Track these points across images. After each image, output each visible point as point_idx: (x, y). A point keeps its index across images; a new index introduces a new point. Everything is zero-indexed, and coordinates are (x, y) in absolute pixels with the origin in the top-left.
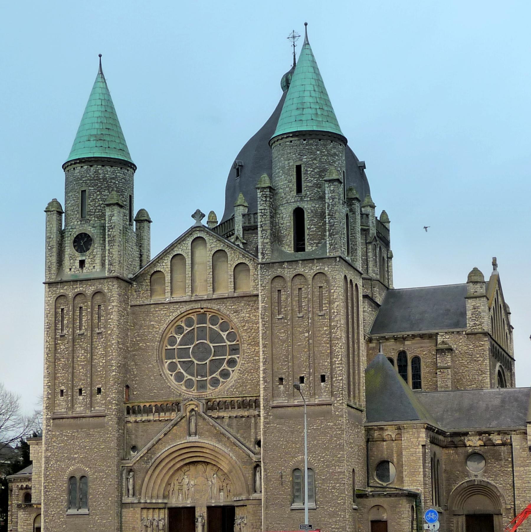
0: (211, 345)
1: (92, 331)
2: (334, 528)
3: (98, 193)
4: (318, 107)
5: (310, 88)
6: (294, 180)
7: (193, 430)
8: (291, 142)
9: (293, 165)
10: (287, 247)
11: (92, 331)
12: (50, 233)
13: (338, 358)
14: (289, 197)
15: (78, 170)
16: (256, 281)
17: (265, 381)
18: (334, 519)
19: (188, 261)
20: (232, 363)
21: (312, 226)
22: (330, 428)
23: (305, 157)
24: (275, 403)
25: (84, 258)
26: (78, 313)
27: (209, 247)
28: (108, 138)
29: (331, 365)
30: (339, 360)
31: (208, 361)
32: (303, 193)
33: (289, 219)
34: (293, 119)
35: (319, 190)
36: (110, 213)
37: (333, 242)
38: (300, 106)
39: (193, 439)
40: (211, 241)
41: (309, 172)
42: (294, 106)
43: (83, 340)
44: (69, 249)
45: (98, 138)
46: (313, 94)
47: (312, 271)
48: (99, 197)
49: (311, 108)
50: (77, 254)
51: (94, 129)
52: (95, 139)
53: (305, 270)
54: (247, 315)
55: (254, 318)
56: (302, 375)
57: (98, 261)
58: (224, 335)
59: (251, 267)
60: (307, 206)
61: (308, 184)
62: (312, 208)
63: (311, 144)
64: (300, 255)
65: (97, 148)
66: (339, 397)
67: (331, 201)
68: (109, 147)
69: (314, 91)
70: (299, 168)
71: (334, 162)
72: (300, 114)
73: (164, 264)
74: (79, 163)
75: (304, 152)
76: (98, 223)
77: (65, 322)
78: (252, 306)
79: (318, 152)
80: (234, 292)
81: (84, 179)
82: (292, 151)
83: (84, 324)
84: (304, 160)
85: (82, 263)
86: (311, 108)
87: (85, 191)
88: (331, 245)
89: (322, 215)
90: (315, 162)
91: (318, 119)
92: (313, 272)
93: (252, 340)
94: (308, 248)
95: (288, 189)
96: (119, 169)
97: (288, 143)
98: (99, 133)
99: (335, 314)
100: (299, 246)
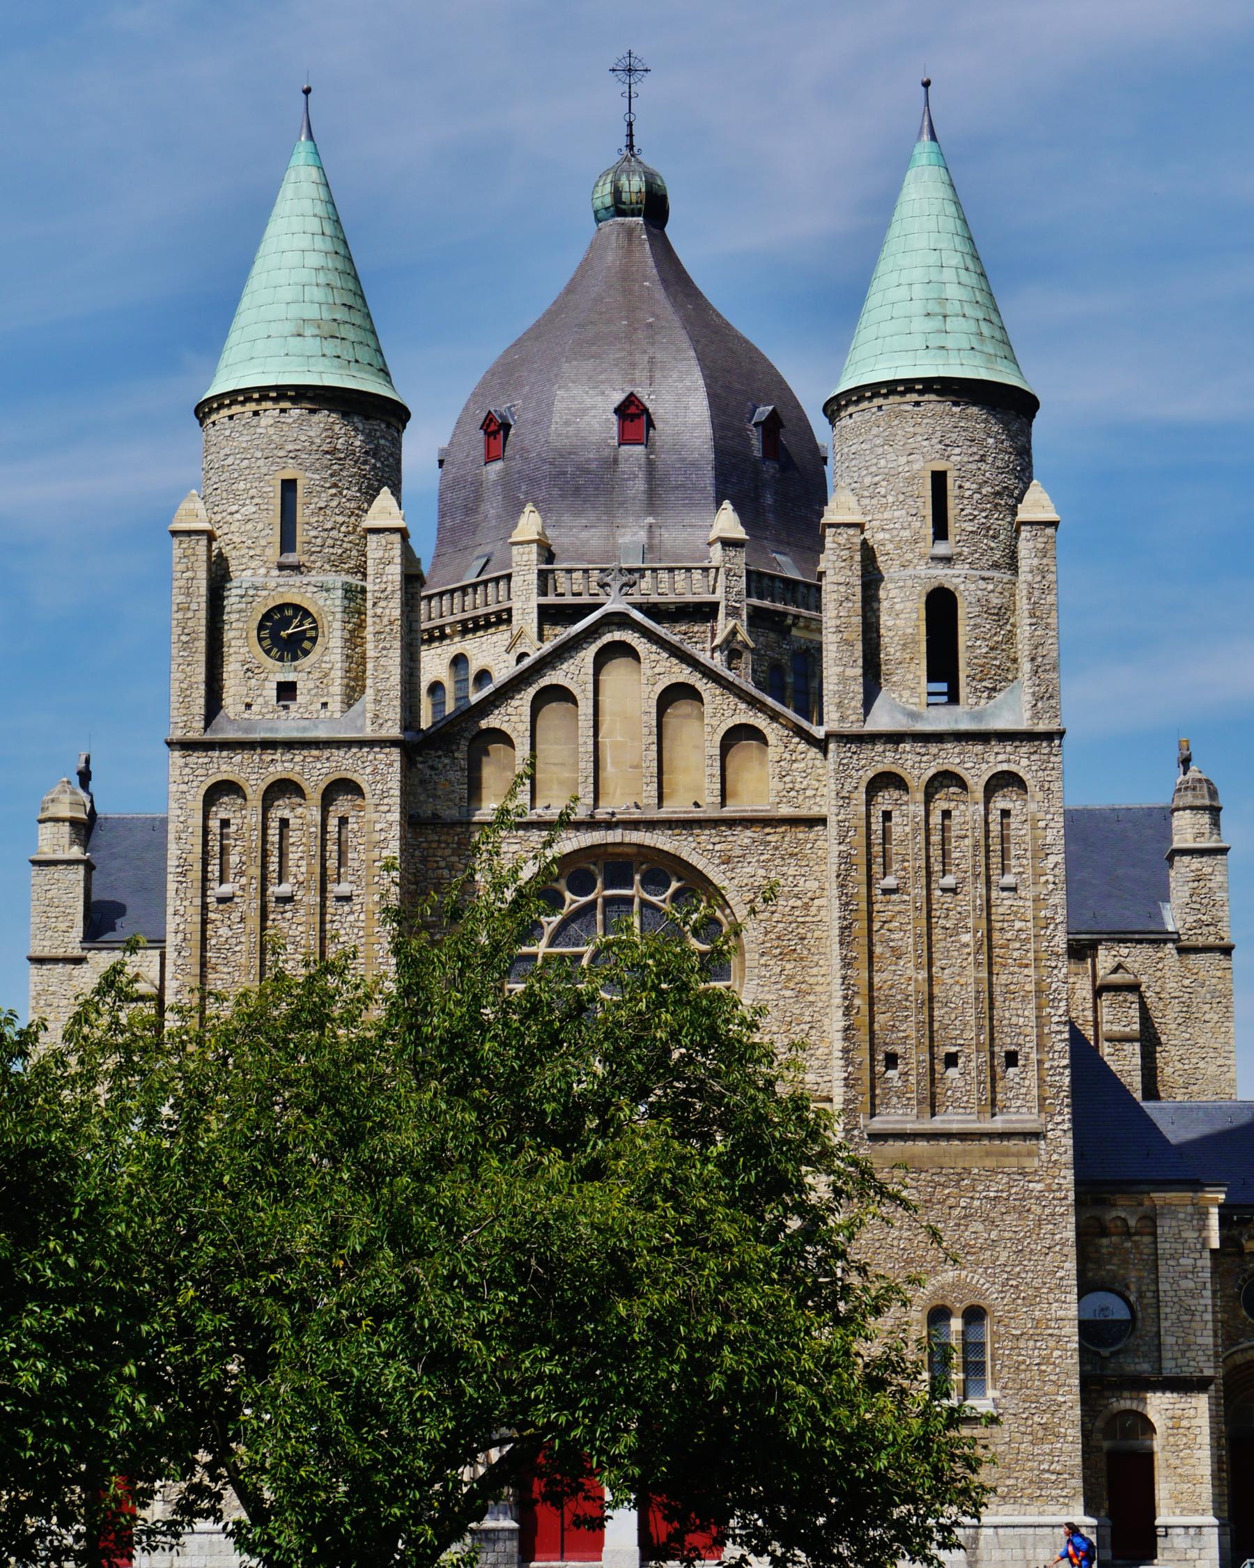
1: (323, 890)
2: (1048, 1471)
3: (333, 491)
4: (981, 316)
6: (928, 512)
8: (917, 404)
9: (923, 469)
10: (906, 694)
11: (323, 890)
12: (188, 595)
13: (1058, 1008)
14: (909, 556)
16: (787, 779)
17: (848, 1062)
18: (1047, 1448)
19: (586, 707)
21: (978, 643)
22: (1038, 1198)
23: (957, 451)
24: (878, 1124)
25: (291, 677)
26: (274, 837)
27: (649, 672)
29: (1040, 1026)
30: (1060, 1012)
33: (914, 616)
34: (919, 342)
35: (993, 545)
36: (380, 554)
37: (1043, 689)
38: (933, 307)
40: (653, 657)
41: (968, 493)
42: (917, 307)
43: (288, 915)
45: (326, 330)
47: (984, 766)
48: (334, 504)
49: (964, 316)
50: (269, 663)
51: (312, 302)
52: (316, 332)
53: (962, 762)
54: (762, 872)
56: (953, 1049)
57: (337, 688)
59: (771, 739)
61: (964, 525)
62: (979, 592)
65: (326, 360)
66: (1060, 1114)
67: (1038, 578)
68: (357, 361)
69: (967, 269)
70: (939, 479)
72: (939, 331)
73: (510, 710)
74: (276, 400)
75: (954, 436)
76: (337, 580)
77: (234, 859)
78: (776, 848)
79: (991, 441)
80: (723, 804)
81: (290, 447)
82: (918, 430)
83: (294, 870)
84: (953, 458)
85: (287, 691)
86: (964, 316)
87: (294, 481)
89: (1002, 614)
90: (984, 466)
91: (986, 350)
93: (775, 943)
95: (906, 534)
96: (383, 426)
97: (909, 408)
98: (327, 315)
99: (1051, 887)
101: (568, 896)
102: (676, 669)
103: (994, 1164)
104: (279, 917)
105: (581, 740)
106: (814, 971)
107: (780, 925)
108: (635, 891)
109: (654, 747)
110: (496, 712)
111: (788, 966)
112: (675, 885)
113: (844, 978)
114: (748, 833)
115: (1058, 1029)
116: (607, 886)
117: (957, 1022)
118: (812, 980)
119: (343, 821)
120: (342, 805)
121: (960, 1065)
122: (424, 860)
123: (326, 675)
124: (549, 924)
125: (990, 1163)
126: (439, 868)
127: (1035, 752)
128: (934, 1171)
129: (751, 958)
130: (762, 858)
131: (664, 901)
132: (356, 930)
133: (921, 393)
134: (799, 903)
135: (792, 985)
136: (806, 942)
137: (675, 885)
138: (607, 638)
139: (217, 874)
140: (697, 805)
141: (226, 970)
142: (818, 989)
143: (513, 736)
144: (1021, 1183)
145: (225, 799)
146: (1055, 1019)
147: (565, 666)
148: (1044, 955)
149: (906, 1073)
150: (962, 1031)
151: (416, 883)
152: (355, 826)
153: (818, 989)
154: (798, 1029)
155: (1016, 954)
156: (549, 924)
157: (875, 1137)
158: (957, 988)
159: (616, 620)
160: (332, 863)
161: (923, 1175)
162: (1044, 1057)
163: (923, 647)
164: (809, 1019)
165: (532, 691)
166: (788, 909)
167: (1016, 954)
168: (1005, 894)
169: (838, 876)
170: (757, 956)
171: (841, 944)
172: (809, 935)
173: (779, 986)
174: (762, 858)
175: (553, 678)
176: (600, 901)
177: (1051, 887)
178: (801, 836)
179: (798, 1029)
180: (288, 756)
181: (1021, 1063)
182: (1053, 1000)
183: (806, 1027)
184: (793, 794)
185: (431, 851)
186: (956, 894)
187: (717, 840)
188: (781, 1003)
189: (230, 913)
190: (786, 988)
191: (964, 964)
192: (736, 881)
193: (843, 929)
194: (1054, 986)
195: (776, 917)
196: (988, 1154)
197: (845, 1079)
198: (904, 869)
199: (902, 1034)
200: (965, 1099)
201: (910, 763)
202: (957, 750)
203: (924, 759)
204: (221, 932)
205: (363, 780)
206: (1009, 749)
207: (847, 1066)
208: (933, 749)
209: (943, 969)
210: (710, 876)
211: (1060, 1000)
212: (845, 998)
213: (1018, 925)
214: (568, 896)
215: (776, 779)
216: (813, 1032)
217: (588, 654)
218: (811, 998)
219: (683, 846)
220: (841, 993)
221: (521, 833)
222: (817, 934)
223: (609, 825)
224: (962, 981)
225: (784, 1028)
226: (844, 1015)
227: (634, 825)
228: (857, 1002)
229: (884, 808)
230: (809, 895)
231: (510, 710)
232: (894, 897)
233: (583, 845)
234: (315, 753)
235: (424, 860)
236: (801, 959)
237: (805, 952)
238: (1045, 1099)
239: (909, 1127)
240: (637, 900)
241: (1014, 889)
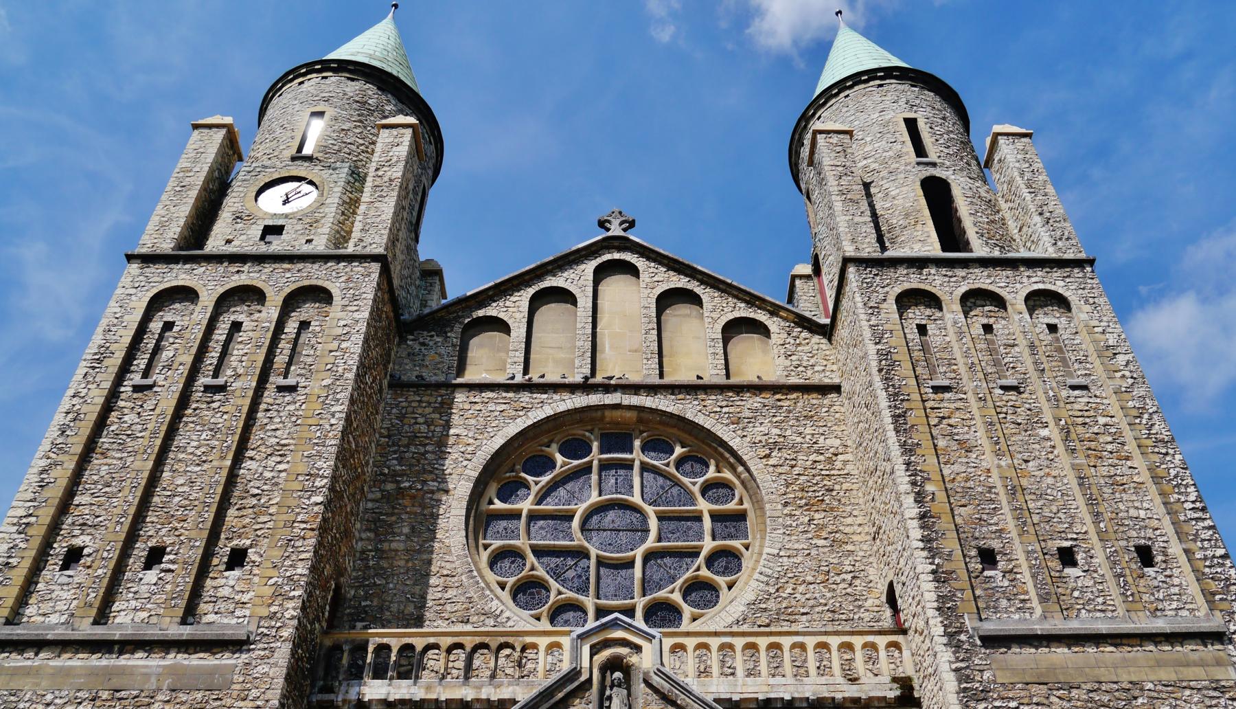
0: (650, 510)
13: (1187, 494)
16: (793, 358)
17: (933, 553)
20: (726, 560)
24: (992, 626)
27: (648, 280)
30: (1192, 497)
31: (639, 553)
54: (777, 431)
55: (799, 439)
58: (694, 484)
73: (508, 304)
83: (234, 364)
99: (1130, 381)
101: (559, 459)
102: (674, 278)
103: (1173, 677)
104: (204, 406)
105: (579, 326)
106: (849, 520)
107: (802, 478)
108: (637, 455)
109: (655, 332)
110: (494, 304)
111: (817, 516)
112: (679, 450)
113: (908, 464)
114: (758, 399)
115: (1196, 515)
116: (602, 452)
117: (1060, 515)
118: (847, 530)
119: (304, 325)
120: (307, 311)
121: (1081, 562)
122: (402, 417)
123: (316, 221)
124: (537, 483)
125: (1167, 675)
126: (416, 423)
127: (1069, 276)
128: (1089, 686)
129: (773, 508)
130: (775, 420)
131: (668, 465)
132: (294, 419)
133: (881, 78)
134: (821, 458)
135: (824, 534)
136: (834, 493)
137: (679, 450)
138: (607, 257)
139: (143, 367)
140: (699, 377)
141: (119, 455)
142: (855, 538)
143: (510, 322)
144: (1222, 701)
145: (177, 306)
146: (1188, 505)
147: (565, 274)
148: (1149, 442)
149: (1011, 571)
150: (1071, 524)
151: (389, 436)
152: (318, 329)
153: (855, 538)
154: (838, 579)
155: (1109, 447)
156: (537, 483)
157: (991, 641)
158: (1050, 480)
159: (616, 243)
160: (280, 360)
161: (1074, 692)
162: (1191, 545)
163: (927, 212)
164: (850, 568)
165: (531, 291)
166: (809, 463)
167: (1109, 447)
168: (1077, 392)
169: (880, 371)
170: (780, 507)
171: (897, 431)
172: (837, 487)
173: (810, 536)
174: (775, 420)
176: (595, 463)
177: (1130, 381)
178: (814, 402)
179: (838, 579)
180: (257, 268)
181: (1159, 558)
182: (1178, 486)
183: (849, 577)
184: (800, 369)
185: (410, 409)
186: (1020, 393)
187: (724, 403)
188: (814, 552)
189: (145, 401)
190: (819, 537)
191: (1051, 456)
192: (748, 439)
193: (896, 417)
194: (1173, 472)
195: (797, 470)
196: (1159, 664)
197: (933, 572)
198: (954, 371)
199: (994, 528)
200: (1100, 600)
201: (938, 282)
202: (985, 273)
203: (953, 279)
204: (127, 415)
205: (335, 288)
206: (1040, 273)
207: (933, 557)
208: (961, 272)
209: (1026, 461)
210: (719, 434)
211: (1187, 486)
212: (914, 484)
213: (1102, 420)
214: (559, 459)
215: (783, 357)
216: (857, 582)
217: (590, 267)
218: (850, 547)
219: (690, 409)
220: (908, 479)
221: (511, 395)
222: (845, 486)
223: (607, 388)
224: (1054, 473)
225: (821, 578)
226: (916, 501)
227: (635, 389)
228: (929, 488)
229: (918, 322)
230: (832, 450)
231: (508, 304)
232: (947, 395)
233: (578, 406)
234: (286, 266)
235: (402, 417)
236: (832, 509)
237: (836, 504)
238: (1213, 594)
239: (1039, 628)
240: (637, 464)
241: (1085, 388)
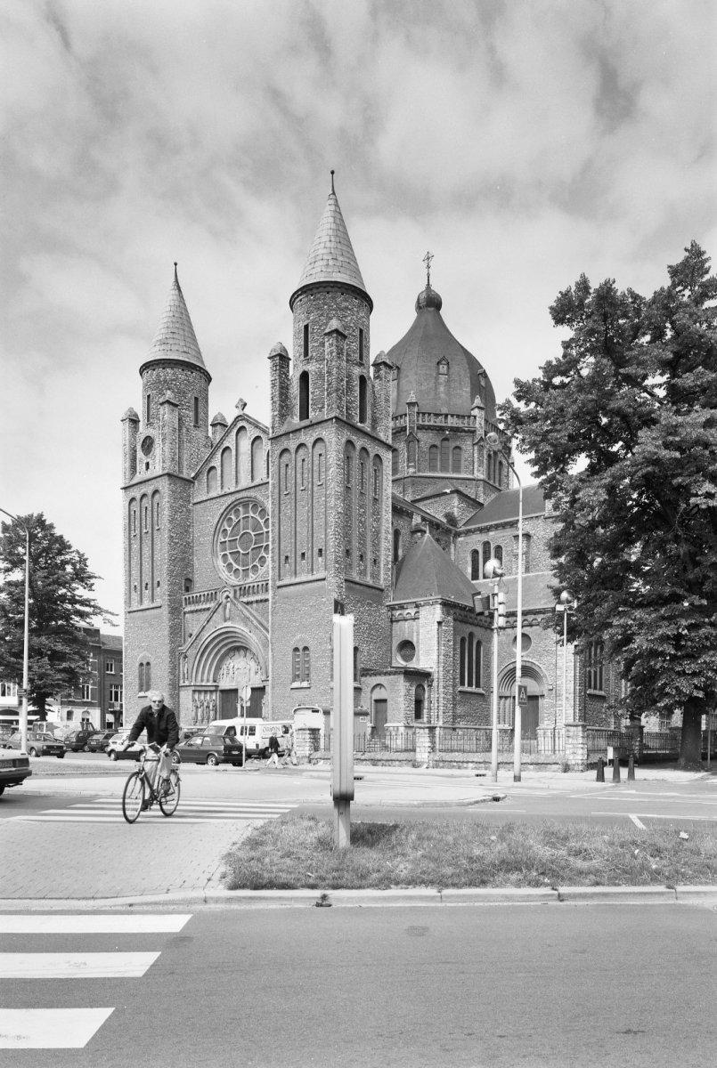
5: (327, 239)
7: (228, 616)
8: (301, 300)
15: (152, 375)
24: (281, 583)
28: (171, 341)
32: (310, 355)
39: (229, 624)
44: (140, 454)
46: (328, 244)
60: (312, 368)
63: (319, 299)
64: (306, 422)
70: (306, 327)
71: (346, 317)
88: (328, 406)
90: (322, 318)
92: (313, 440)
94: (311, 415)
100: (304, 414)
120: (157, 496)
157: (279, 587)
175: (226, 444)
